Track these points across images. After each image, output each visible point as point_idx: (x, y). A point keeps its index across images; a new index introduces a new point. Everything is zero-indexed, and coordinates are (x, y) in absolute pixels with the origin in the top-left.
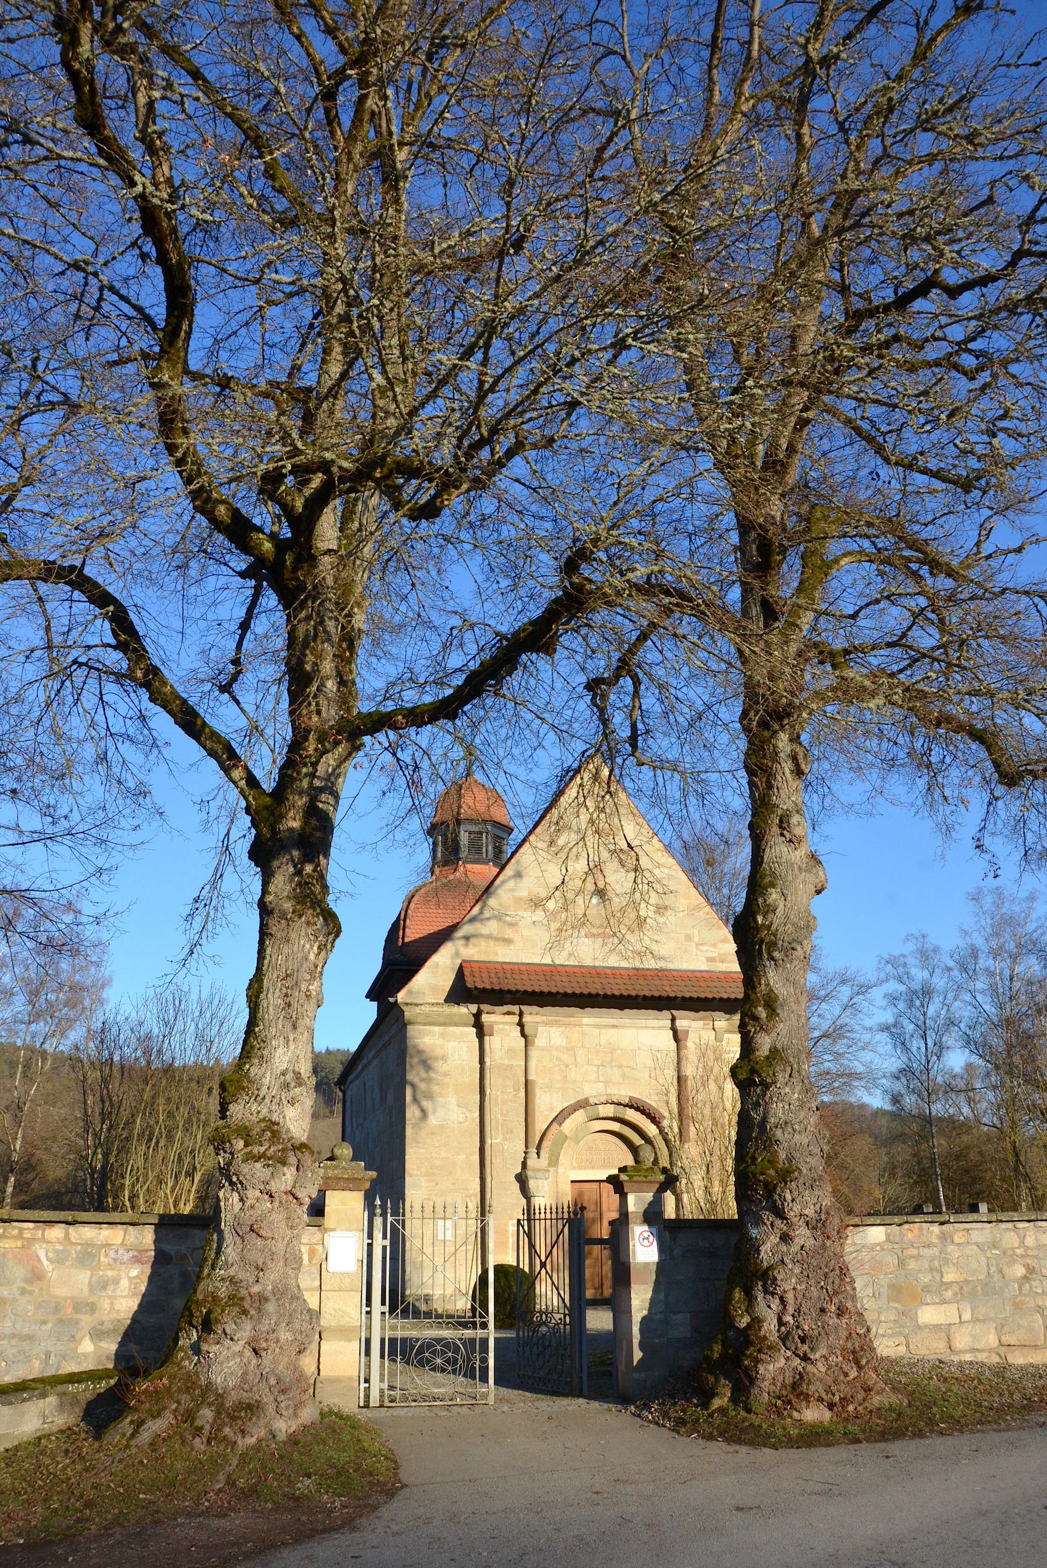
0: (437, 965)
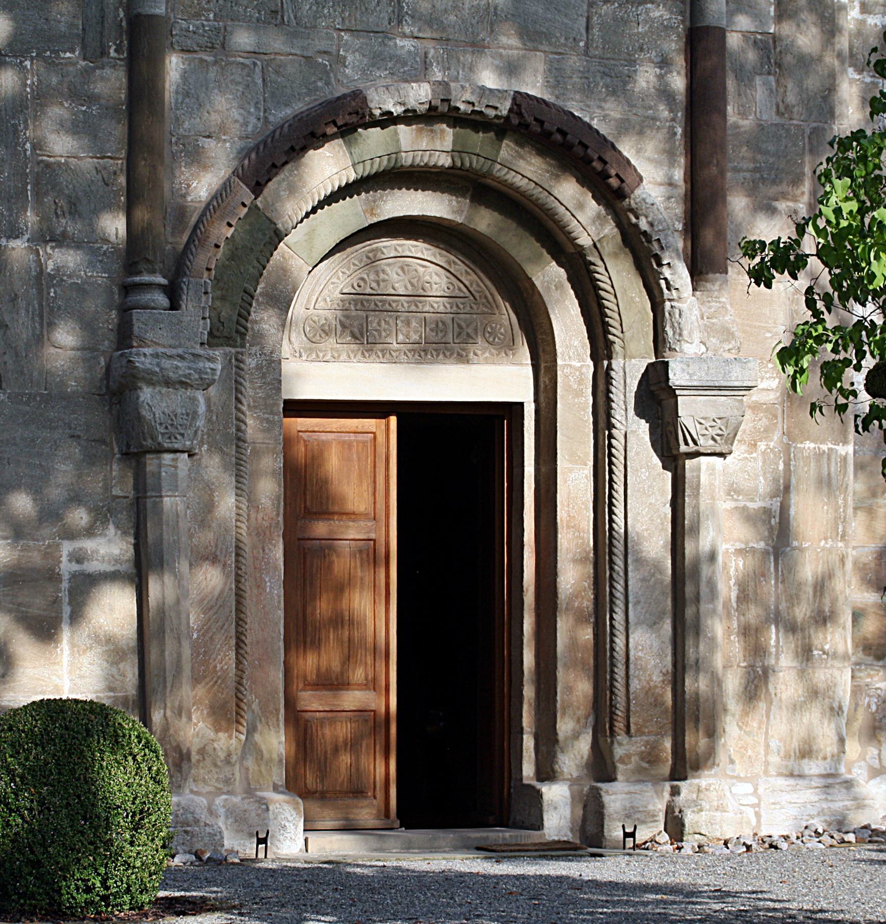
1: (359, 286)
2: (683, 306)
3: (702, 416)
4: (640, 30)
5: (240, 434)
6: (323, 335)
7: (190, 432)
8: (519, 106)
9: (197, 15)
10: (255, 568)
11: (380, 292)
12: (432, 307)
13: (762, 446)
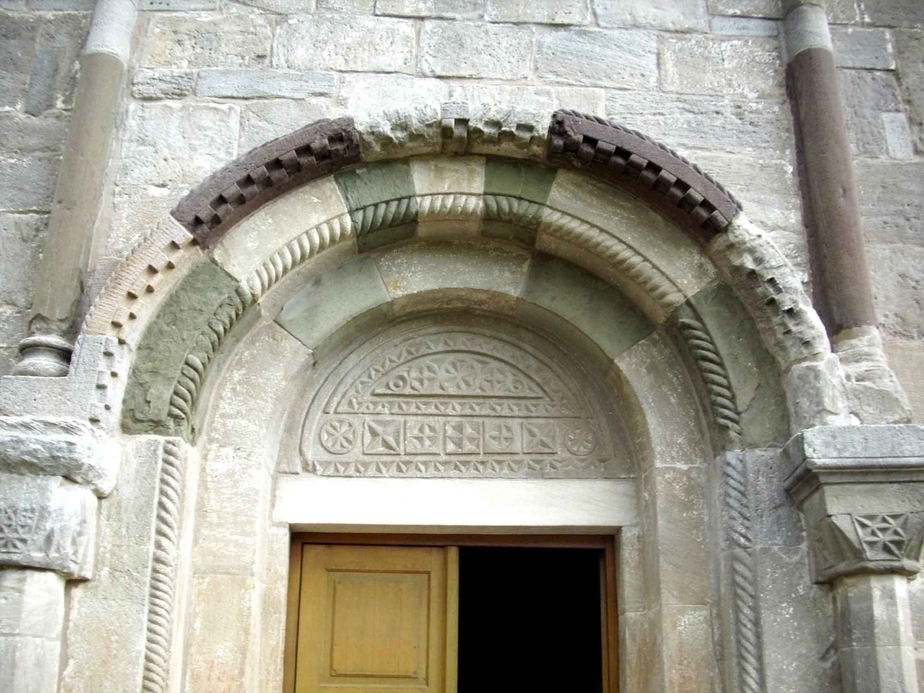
2: (821, 365)
3: (865, 512)
4: (726, 66)
5: (160, 553)
6: (346, 444)
7: (40, 538)
8: (560, 123)
9: (168, 63)
11: (423, 392)
12: (494, 409)
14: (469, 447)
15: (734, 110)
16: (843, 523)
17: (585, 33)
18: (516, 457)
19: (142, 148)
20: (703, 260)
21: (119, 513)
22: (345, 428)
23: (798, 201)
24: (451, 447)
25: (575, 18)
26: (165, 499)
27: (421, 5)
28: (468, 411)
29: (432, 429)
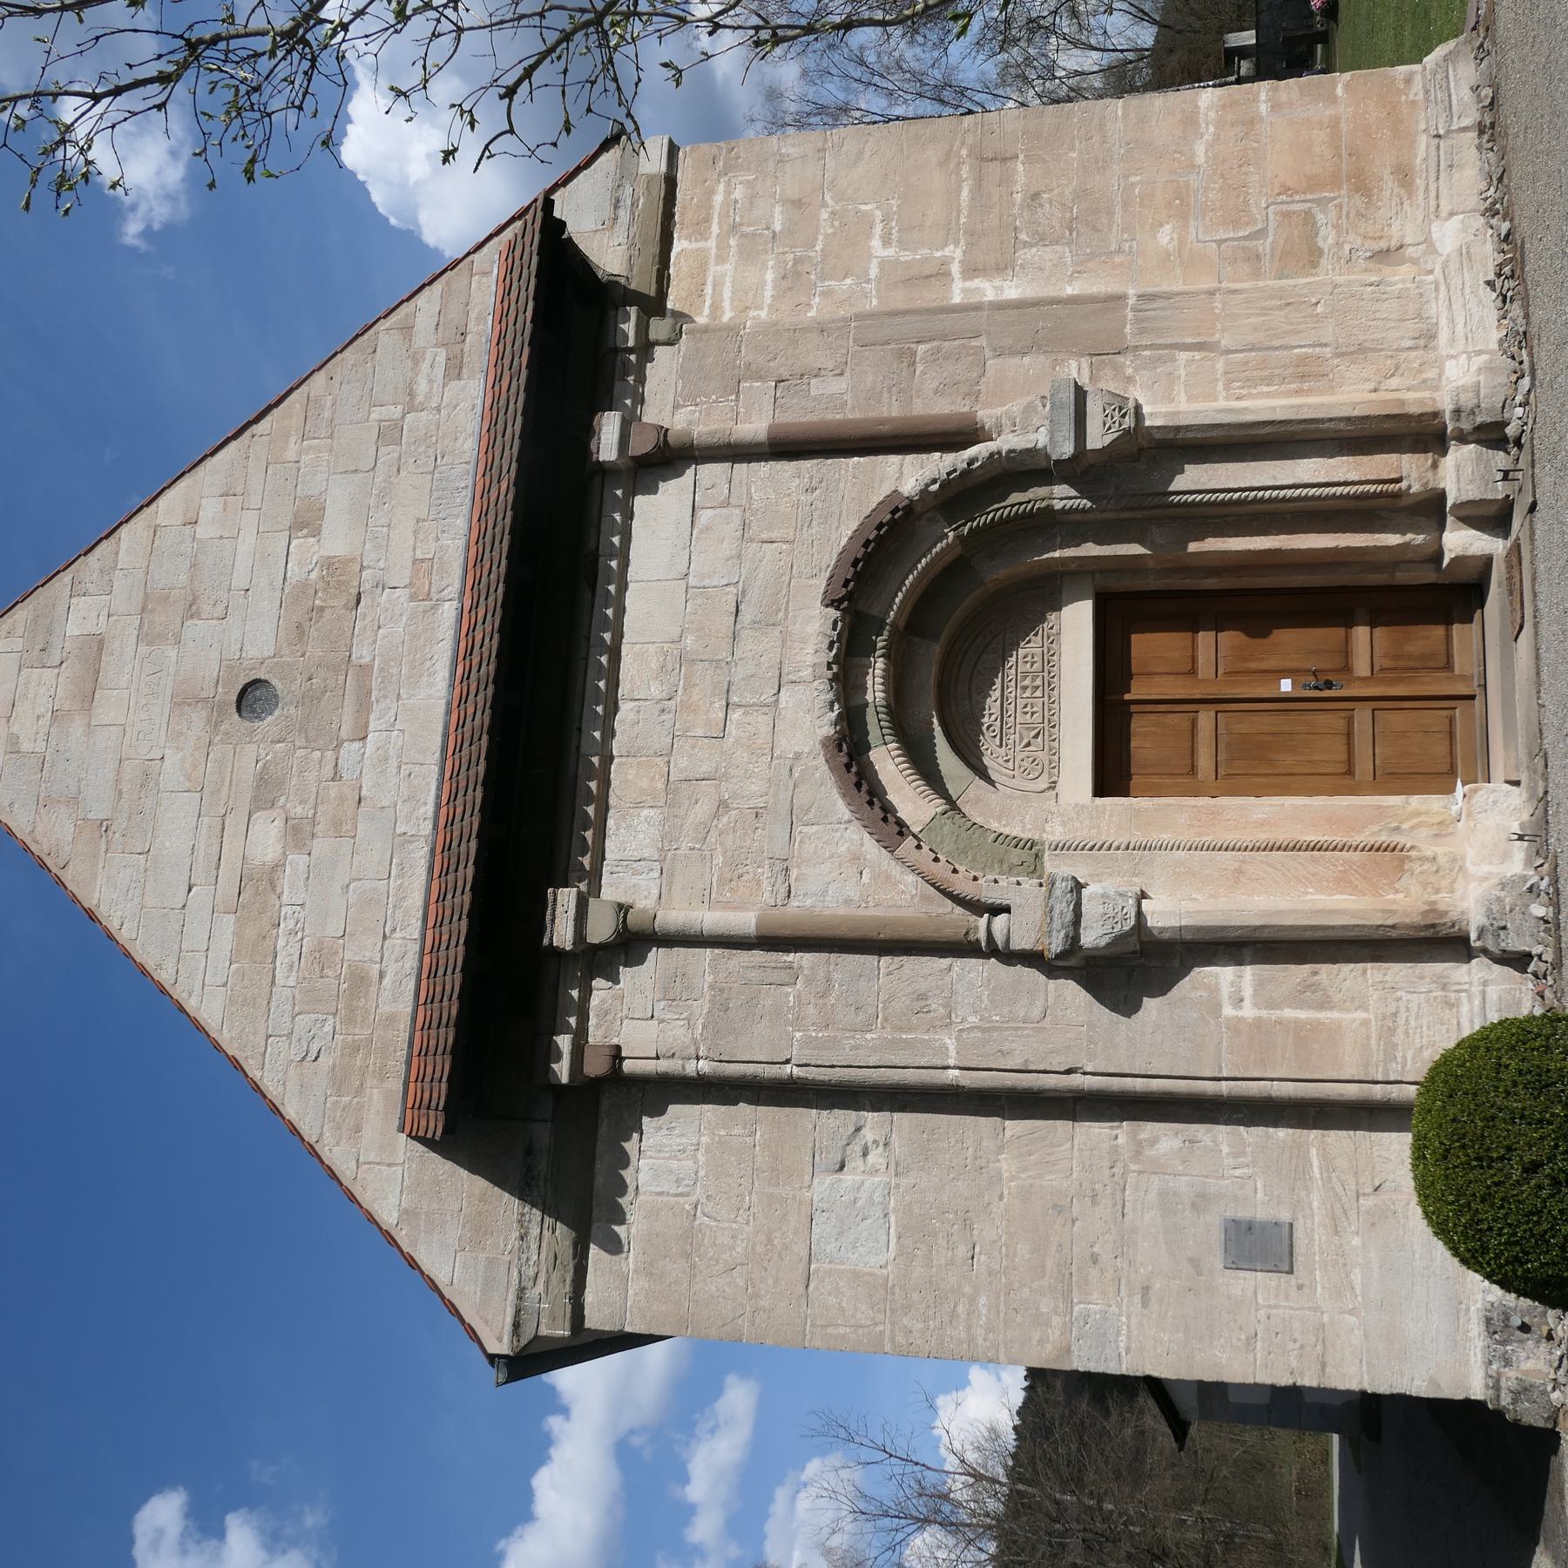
0: (407, 1214)
1: (994, 731)
8: (833, 601)
9: (759, 883)
10: (1245, 828)
13: (1129, 371)
14: (1038, 682)
15: (809, 494)
16: (1108, 439)
17: (744, 592)
18: (1045, 651)
19: (830, 892)
20: (924, 518)
21: (1097, 875)
22: (1025, 763)
23: (881, 458)
24: (1039, 693)
25: (731, 599)
26: (1087, 847)
27: (717, 705)
28: (1013, 683)
29: (1025, 706)
